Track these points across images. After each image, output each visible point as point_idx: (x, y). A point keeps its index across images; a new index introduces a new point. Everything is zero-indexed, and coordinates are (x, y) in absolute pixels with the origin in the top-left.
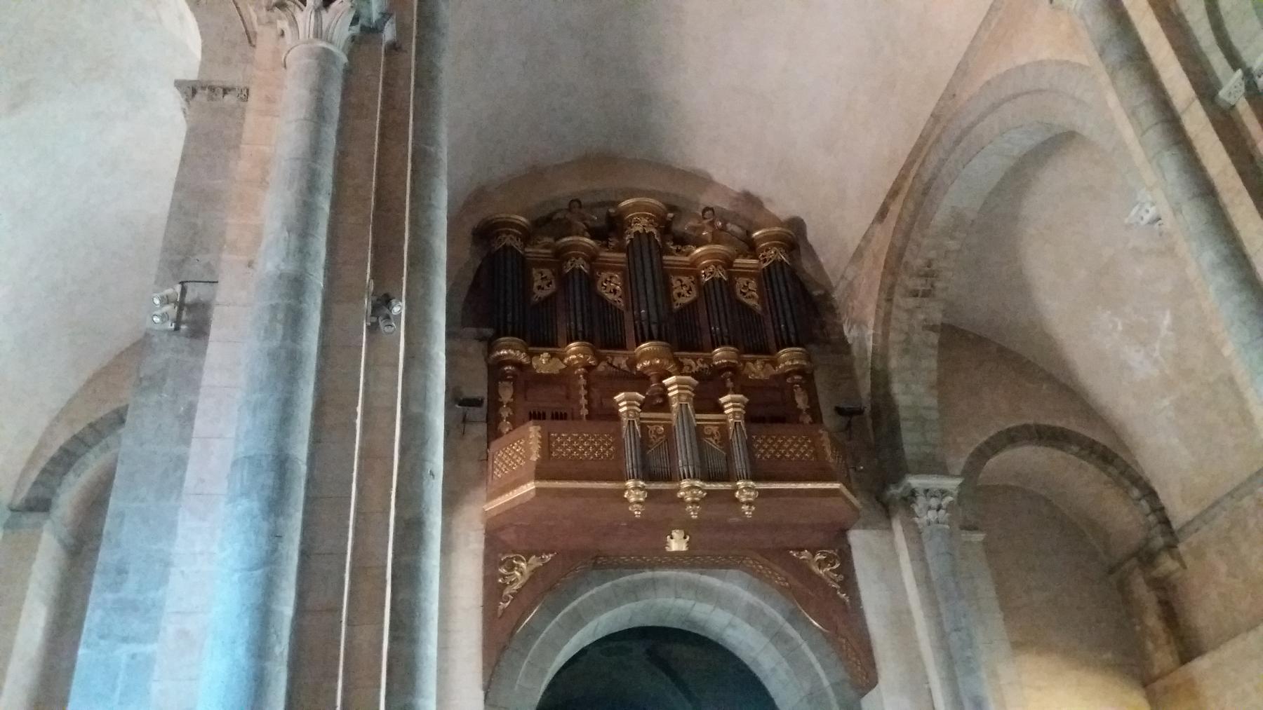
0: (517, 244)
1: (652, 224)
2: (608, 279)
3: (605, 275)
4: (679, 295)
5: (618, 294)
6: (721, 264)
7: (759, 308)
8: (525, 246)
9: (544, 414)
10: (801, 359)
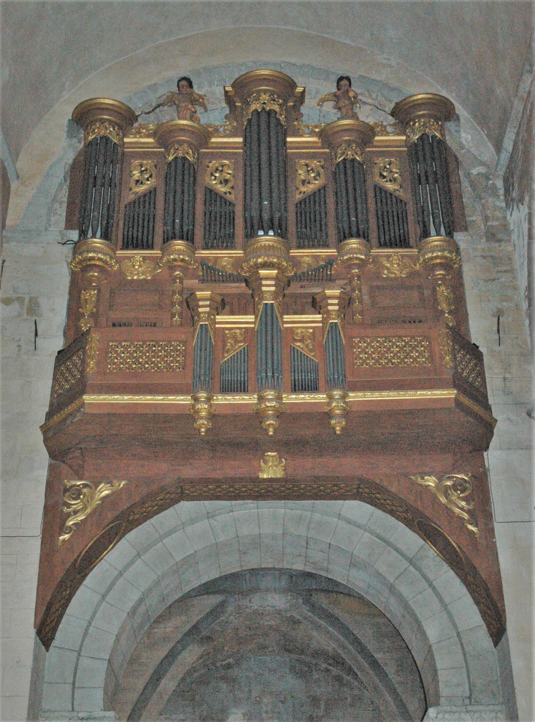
0: (110, 132)
1: (274, 100)
2: (220, 169)
3: (214, 164)
4: (304, 182)
5: (230, 185)
6: (353, 141)
7: (401, 194)
8: (124, 136)
9: (18, 346)
10: (443, 250)
